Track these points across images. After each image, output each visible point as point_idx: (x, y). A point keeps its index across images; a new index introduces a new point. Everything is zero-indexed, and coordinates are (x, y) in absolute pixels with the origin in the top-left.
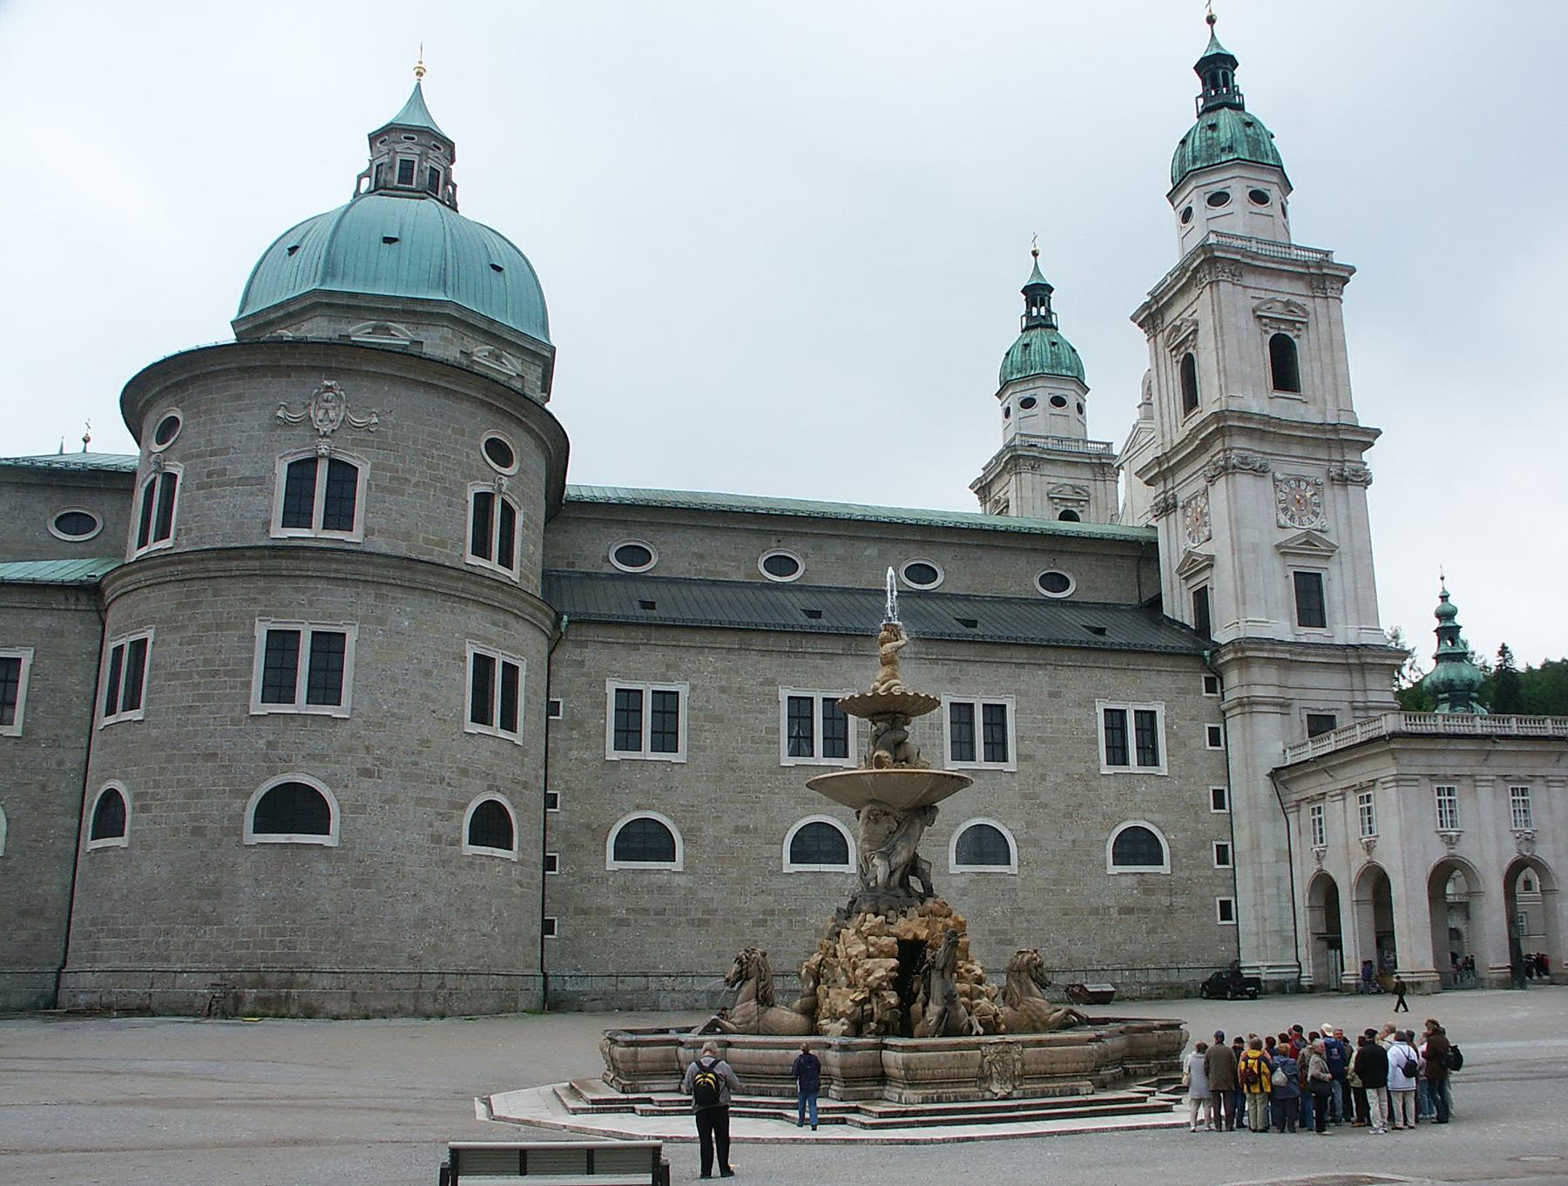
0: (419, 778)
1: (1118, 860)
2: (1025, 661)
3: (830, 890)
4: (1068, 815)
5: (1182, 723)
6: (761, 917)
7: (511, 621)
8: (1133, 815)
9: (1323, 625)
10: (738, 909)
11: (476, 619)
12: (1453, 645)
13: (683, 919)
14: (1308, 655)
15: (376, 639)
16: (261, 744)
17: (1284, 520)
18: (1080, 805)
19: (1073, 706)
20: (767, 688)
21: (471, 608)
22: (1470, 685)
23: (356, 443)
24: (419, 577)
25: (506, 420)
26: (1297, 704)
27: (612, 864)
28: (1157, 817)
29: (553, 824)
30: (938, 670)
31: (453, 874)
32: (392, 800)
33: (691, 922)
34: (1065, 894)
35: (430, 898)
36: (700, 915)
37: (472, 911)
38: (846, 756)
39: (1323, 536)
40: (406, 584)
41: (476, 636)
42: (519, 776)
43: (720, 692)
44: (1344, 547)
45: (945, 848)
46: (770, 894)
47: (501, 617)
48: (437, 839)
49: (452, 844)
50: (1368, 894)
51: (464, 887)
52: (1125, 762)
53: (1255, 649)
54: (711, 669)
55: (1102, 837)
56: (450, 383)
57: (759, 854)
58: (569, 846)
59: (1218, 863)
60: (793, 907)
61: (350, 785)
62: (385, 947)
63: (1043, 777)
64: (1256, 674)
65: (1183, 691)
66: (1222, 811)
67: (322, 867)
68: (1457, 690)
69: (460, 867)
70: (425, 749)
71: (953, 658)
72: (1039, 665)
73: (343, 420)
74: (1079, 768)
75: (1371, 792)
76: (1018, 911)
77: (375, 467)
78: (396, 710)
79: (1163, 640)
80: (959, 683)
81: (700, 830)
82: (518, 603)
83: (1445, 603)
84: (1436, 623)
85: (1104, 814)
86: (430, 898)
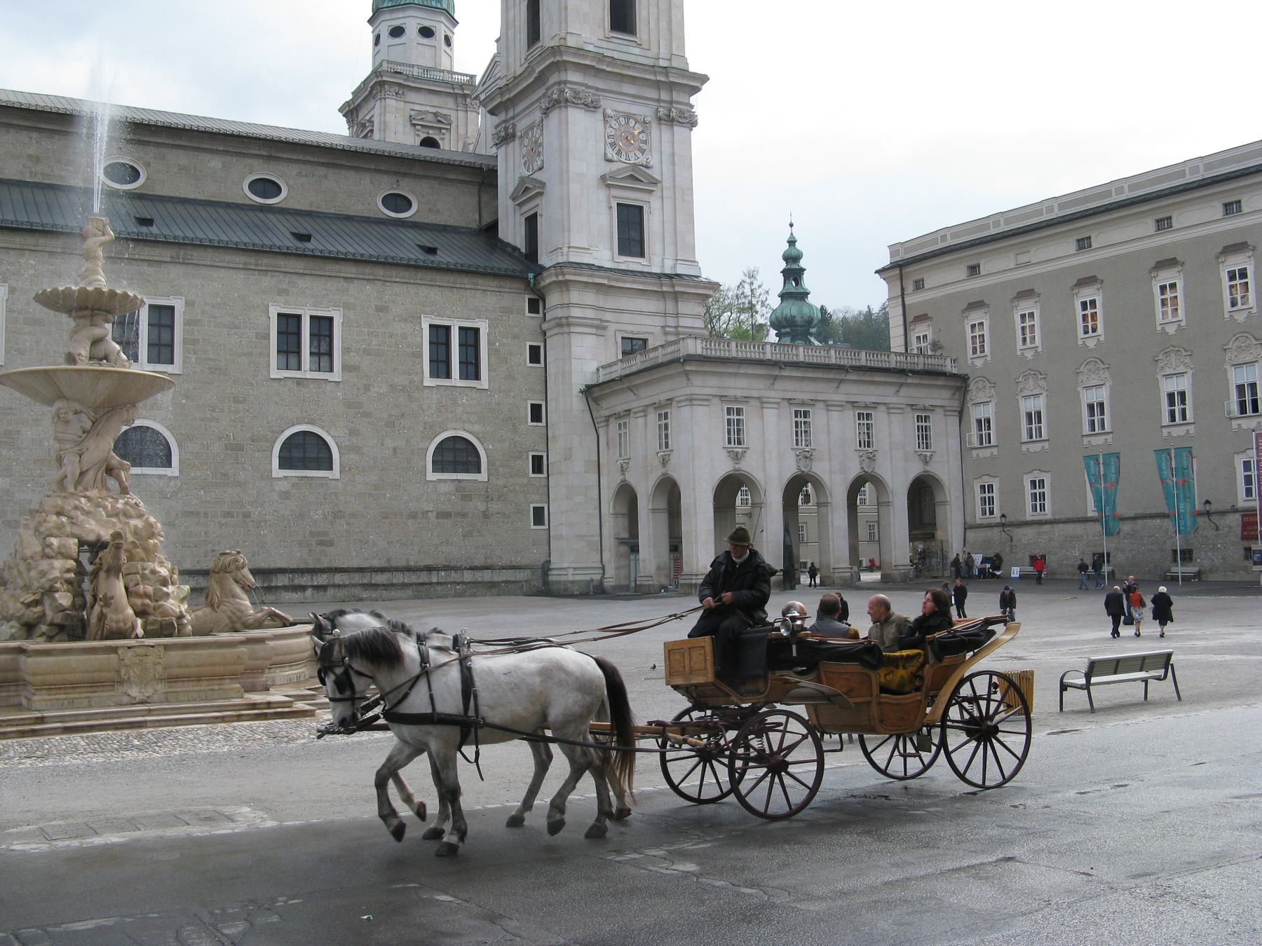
1: (439, 466)
2: (353, 276)
4: (390, 424)
9: (642, 255)
12: (797, 284)
14: (625, 282)
17: (611, 154)
18: (403, 415)
19: (399, 321)
22: (809, 322)
26: (612, 327)
28: (477, 428)
30: (267, 281)
38: (172, 362)
39: (647, 171)
44: (667, 183)
50: (662, 504)
52: (448, 376)
53: (574, 274)
54: (32, 272)
59: (533, 472)
63: (367, 388)
64: (575, 296)
65: (507, 311)
66: (539, 424)
68: (797, 326)
71: (283, 270)
72: (368, 280)
75: (668, 410)
76: (337, 515)
79: (504, 264)
80: (288, 295)
83: (792, 247)
84: (783, 265)
85: (425, 423)
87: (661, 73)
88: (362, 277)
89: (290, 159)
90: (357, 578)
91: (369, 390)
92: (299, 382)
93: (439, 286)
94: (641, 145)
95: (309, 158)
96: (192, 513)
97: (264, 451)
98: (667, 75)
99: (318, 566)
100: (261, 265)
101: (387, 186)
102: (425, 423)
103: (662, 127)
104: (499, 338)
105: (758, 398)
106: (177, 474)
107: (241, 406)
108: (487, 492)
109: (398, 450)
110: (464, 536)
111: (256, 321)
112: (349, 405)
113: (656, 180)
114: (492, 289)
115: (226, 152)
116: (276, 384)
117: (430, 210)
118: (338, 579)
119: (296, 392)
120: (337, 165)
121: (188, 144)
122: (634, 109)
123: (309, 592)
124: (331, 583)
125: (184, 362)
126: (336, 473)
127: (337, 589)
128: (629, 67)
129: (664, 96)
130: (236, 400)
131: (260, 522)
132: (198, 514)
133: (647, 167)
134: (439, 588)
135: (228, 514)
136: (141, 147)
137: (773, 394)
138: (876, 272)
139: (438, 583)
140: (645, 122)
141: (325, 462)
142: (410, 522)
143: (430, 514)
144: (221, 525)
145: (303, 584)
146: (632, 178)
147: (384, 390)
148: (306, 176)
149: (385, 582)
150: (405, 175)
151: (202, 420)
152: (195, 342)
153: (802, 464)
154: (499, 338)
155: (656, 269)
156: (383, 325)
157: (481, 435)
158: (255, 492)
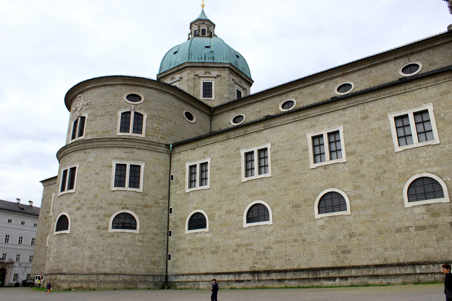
0: (93, 208)
2: (346, 106)
3: (262, 234)
5: (447, 111)
6: (235, 248)
7: (134, 150)
8: (419, 171)
10: (227, 245)
11: (117, 152)
13: (209, 251)
15: (83, 166)
16: (59, 205)
18: (385, 172)
19: (375, 121)
20: (236, 152)
21: (115, 149)
23: (86, 110)
24: (95, 144)
25: (135, 87)
27: (187, 232)
28: (436, 169)
29: (171, 219)
30: (305, 123)
31: (104, 239)
32: (85, 216)
33: (211, 252)
34: (379, 222)
35: (95, 249)
36: (214, 249)
37: (113, 252)
40: (92, 147)
41: (117, 158)
42: (140, 203)
43: (221, 158)
45: (312, 207)
46: (239, 238)
47: (130, 150)
48: (99, 228)
49: (104, 229)
51: (110, 244)
54: (218, 150)
55: (399, 187)
56: (110, 82)
57: (234, 221)
58: (175, 226)
60: (248, 243)
61: (74, 214)
62: (80, 265)
63: (362, 162)
65: (443, 94)
67: (66, 240)
69: (108, 237)
70: (96, 198)
71: (311, 116)
73: (83, 105)
74: (382, 152)
76: (352, 235)
77: (89, 115)
78: (87, 187)
80: (315, 126)
81: (214, 214)
82: (137, 144)
85: (400, 174)
86: (95, 249)
88: (351, 105)
89: (352, 71)
90: (365, 272)
91: (363, 163)
92: (325, 167)
96: (279, 241)
97: (310, 206)
99: (342, 265)
100: (301, 117)
101: (403, 63)
102: (400, 174)
104: (442, 111)
106: (271, 223)
107: (298, 185)
109: (384, 193)
110: (438, 240)
111: (302, 143)
112: (352, 173)
114: (432, 84)
115: (325, 80)
116: (313, 171)
117: (430, 65)
118: (354, 272)
119: (324, 173)
120: (375, 64)
121: (309, 83)
123: (337, 281)
124: (350, 275)
125: (272, 171)
126: (348, 212)
127: (353, 279)
130: (296, 183)
131: (310, 243)
132: (282, 242)
134: (422, 277)
135: (295, 241)
136: (293, 92)
139: (420, 274)
141: (342, 206)
142: (397, 235)
143: (410, 228)
144: (292, 246)
145: (334, 276)
147: (372, 160)
149: (384, 274)
150: (411, 54)
151: (281, 196)
152: (277, 160)
154: (442, 111)
156: (366, 126)
157: (440, 173)
158: (307, 228)
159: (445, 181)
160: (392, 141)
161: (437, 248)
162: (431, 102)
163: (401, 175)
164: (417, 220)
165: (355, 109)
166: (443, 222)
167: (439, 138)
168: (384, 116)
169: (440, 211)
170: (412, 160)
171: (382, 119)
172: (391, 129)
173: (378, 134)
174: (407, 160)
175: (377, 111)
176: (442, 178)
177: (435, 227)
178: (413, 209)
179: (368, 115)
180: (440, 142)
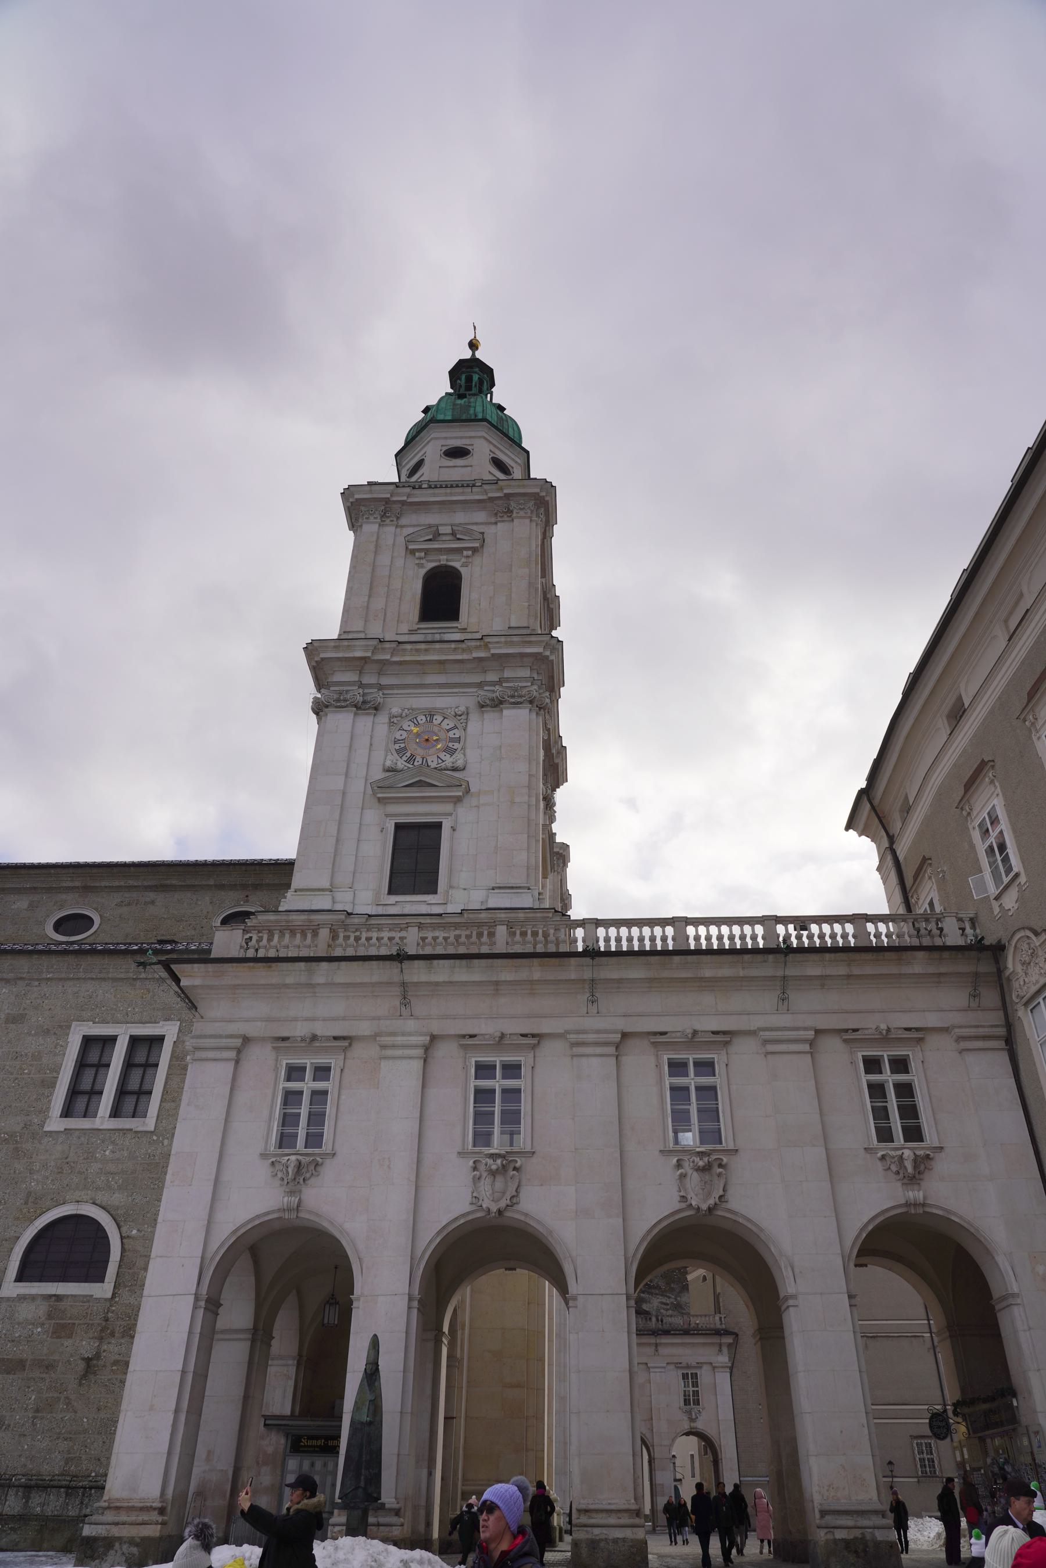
87: (477, 648)
93: (115, 980)
94: (450, 745)
95: (131, 882)
98: (486, 646)
102: (29, 1194)
103: (486, 716)
105: (374, 1037)
108: (107, 1320)
113: (459, 779)
120: (167, 886)
122: (440, 702)
128: (426, 650)
129: (492, 677)
133: (455, 769)
137: (411, 1025)
138: (847, 828)
140: (456, 715)
146: (420, 784)
148: (129, 904)
150: (256, 887)
153: (485, 1187)
155: (450, 908)
159: (123, 1235)
160: (50, 1098)
161: (25, 1435)
162: (178, 1020)
163: (31, 1200)
164: (13, 1341)
165: (4, 990)
166: (72, 1356)
167: (158, 1117)
168: (61, 1027)
169: (77, 1322)
170: (74, 1163)
171: (55, 1034)
172: (62, 1064)
173: (26, 1071)
174: (62, 1159)
175: (53, 1008)
176: (119, 1227)
177: (47, 1367)
178: (18, 1304)
179: (26, 1014)
180: (155, 1129)
